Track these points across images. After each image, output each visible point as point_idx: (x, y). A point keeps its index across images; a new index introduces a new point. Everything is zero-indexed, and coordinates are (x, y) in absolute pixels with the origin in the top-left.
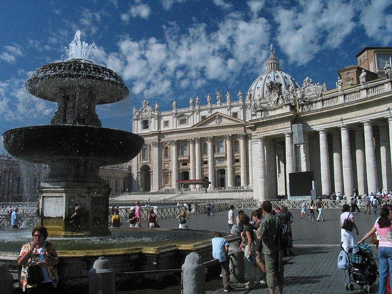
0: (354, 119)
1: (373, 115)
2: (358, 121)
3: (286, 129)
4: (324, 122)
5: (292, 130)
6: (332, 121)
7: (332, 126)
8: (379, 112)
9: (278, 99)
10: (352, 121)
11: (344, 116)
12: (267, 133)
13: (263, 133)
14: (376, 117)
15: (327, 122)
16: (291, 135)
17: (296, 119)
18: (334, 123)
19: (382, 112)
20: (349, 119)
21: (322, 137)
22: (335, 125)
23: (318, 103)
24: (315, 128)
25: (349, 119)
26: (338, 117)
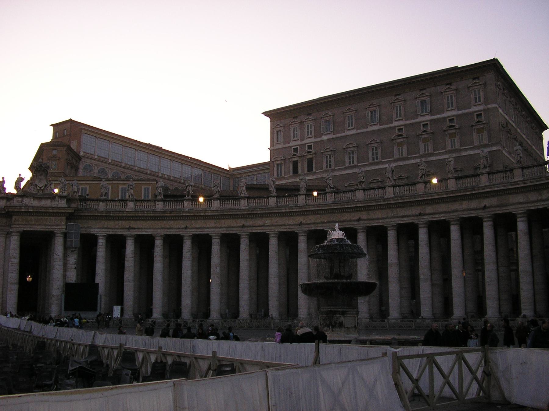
0: (145, 230)
1: (168, 230)
2: (150, 233)
3: (59, 227)
4: (106, 226)
5: (66, 229)
6: (117, 227)
7: (116, 233)
8: (175, 228)
9: (46, 186)
10: (143, 232)
11: (133, 224)
12: (29, 226)
13: (21, 226)
14: (171, 233)
15: (109, 226)
16: (65, 236)
17: (71, 217)
18: (119, 230)
19: (179, 228)
20: (138, 228)
21: (101, 242)
22: (120, 232)
23: (101, 203)
24: (94, 231)
25: (138, 228)
26: (126, 224)
